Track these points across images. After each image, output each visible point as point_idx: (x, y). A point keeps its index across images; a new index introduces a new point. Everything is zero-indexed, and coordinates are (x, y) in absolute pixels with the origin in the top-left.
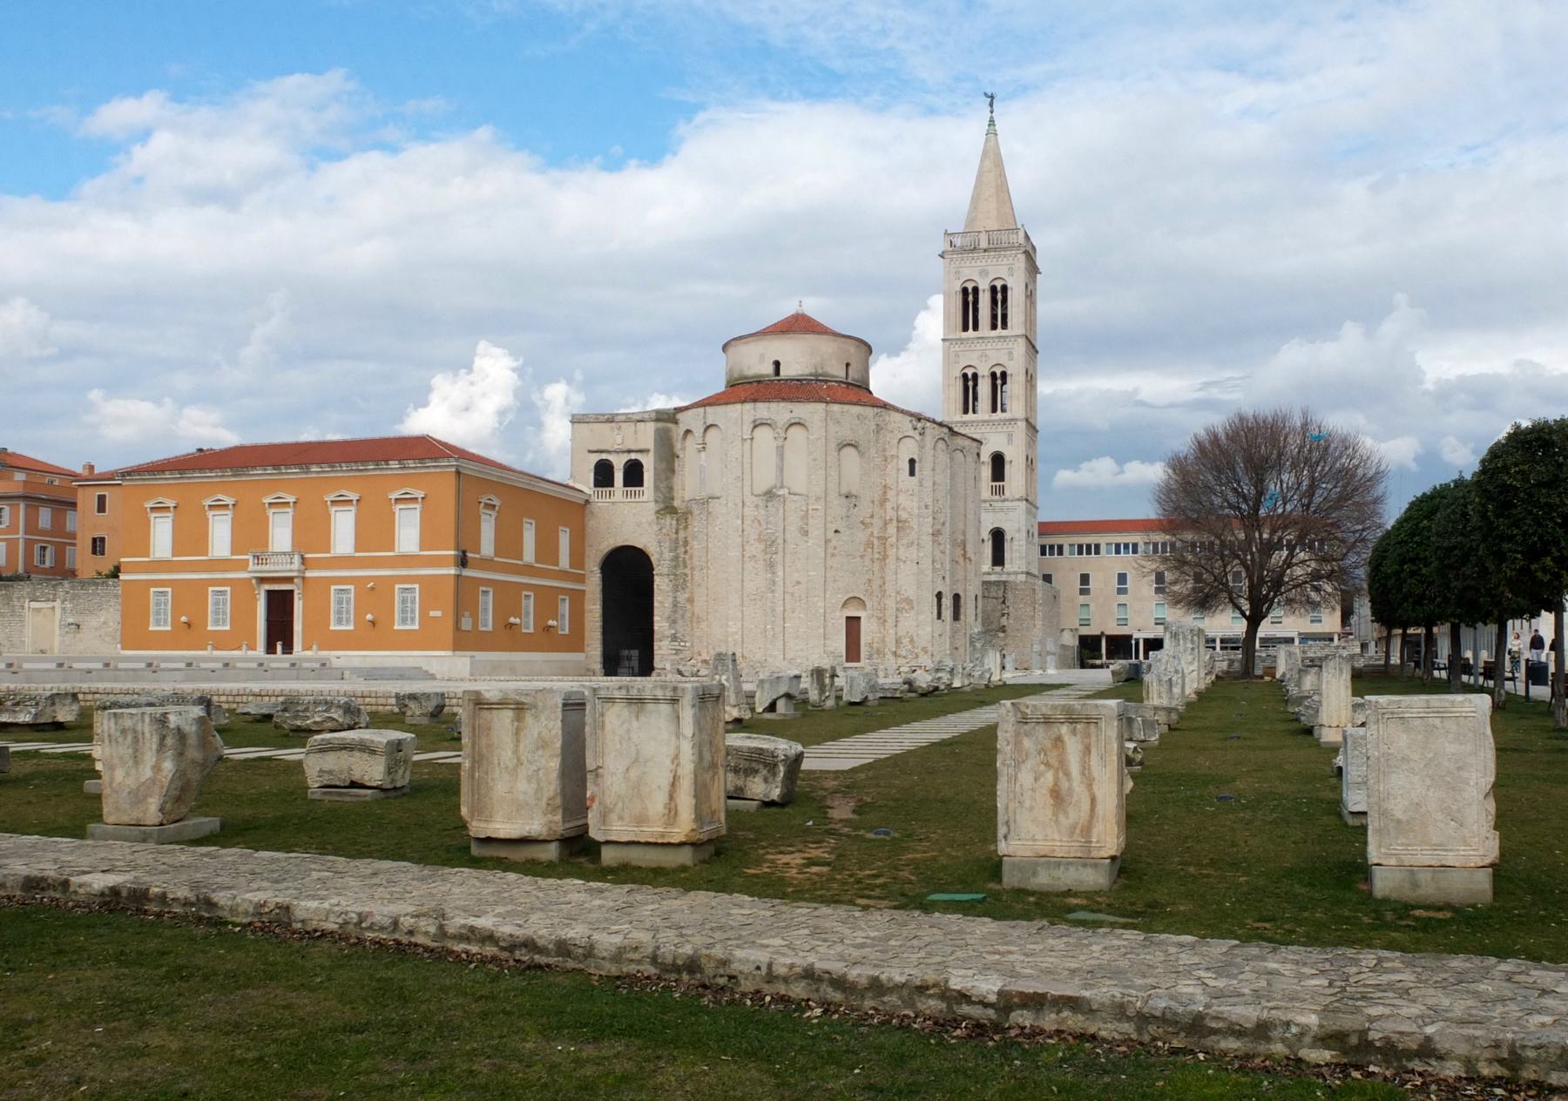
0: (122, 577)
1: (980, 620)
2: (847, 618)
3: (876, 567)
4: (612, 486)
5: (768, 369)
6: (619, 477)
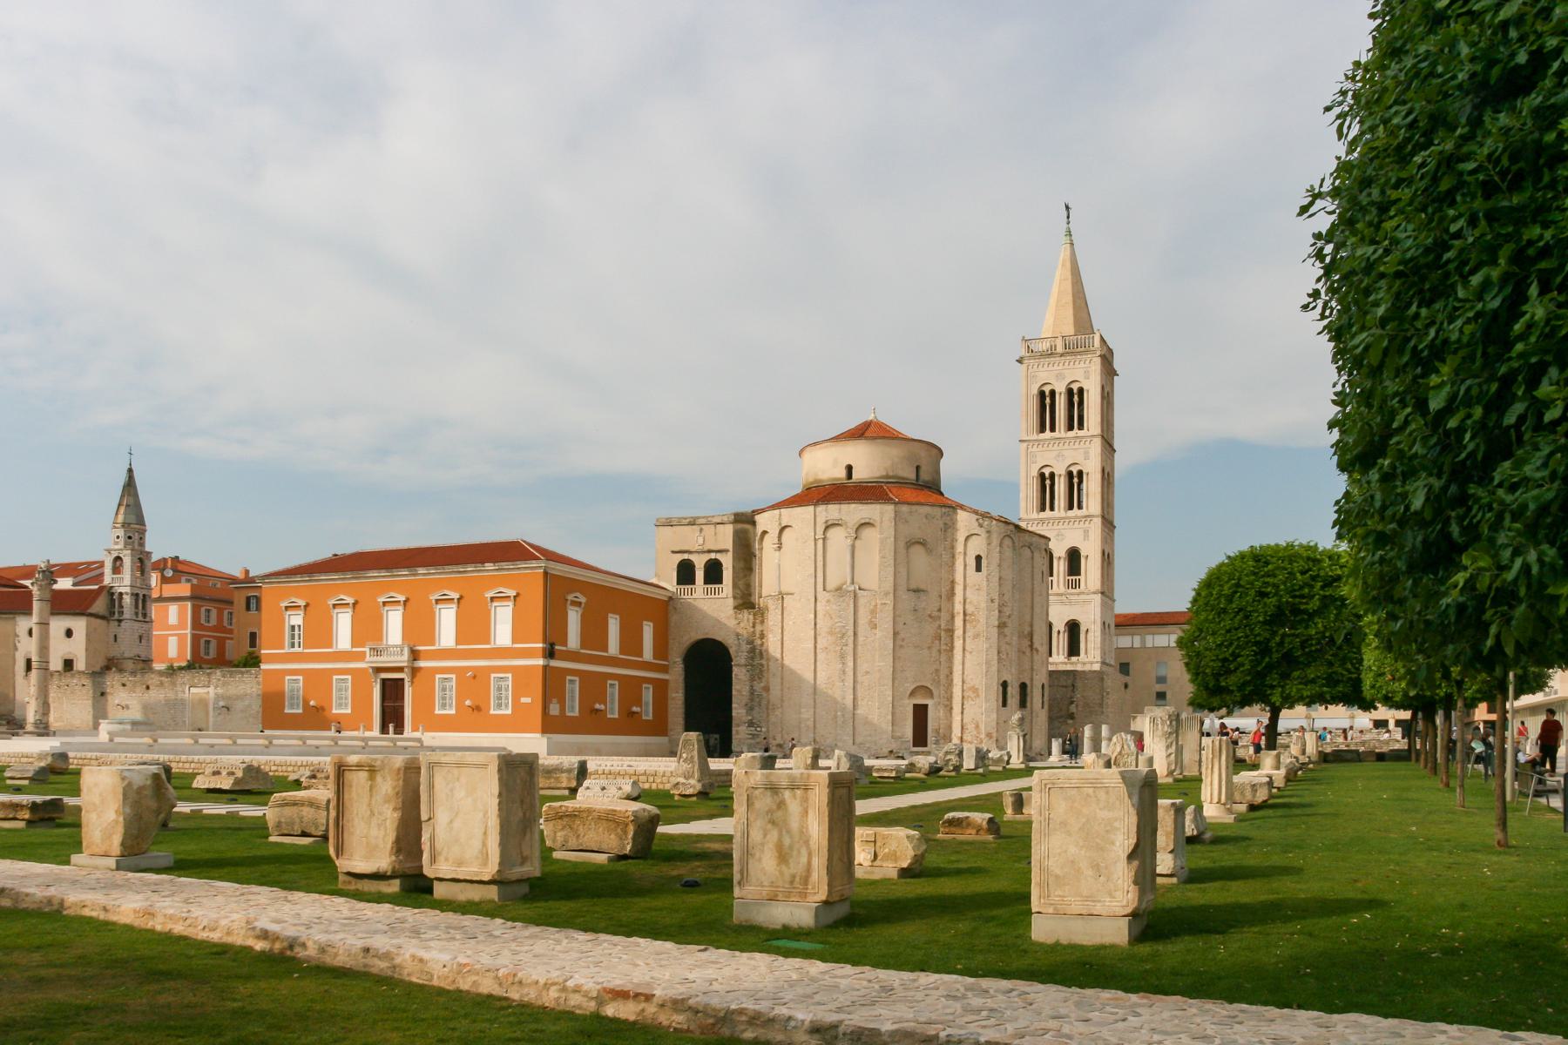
0: (263, 666)
1: (1046, 706)
2: (915, 706)
3: (943, 658)
4: (694, 583)
5: (842, 474)
6: (700, 575)
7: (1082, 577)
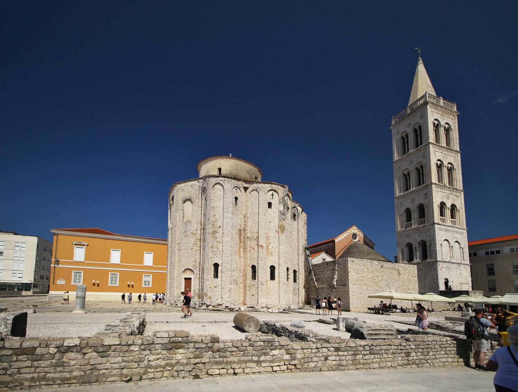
7: (426, 218)
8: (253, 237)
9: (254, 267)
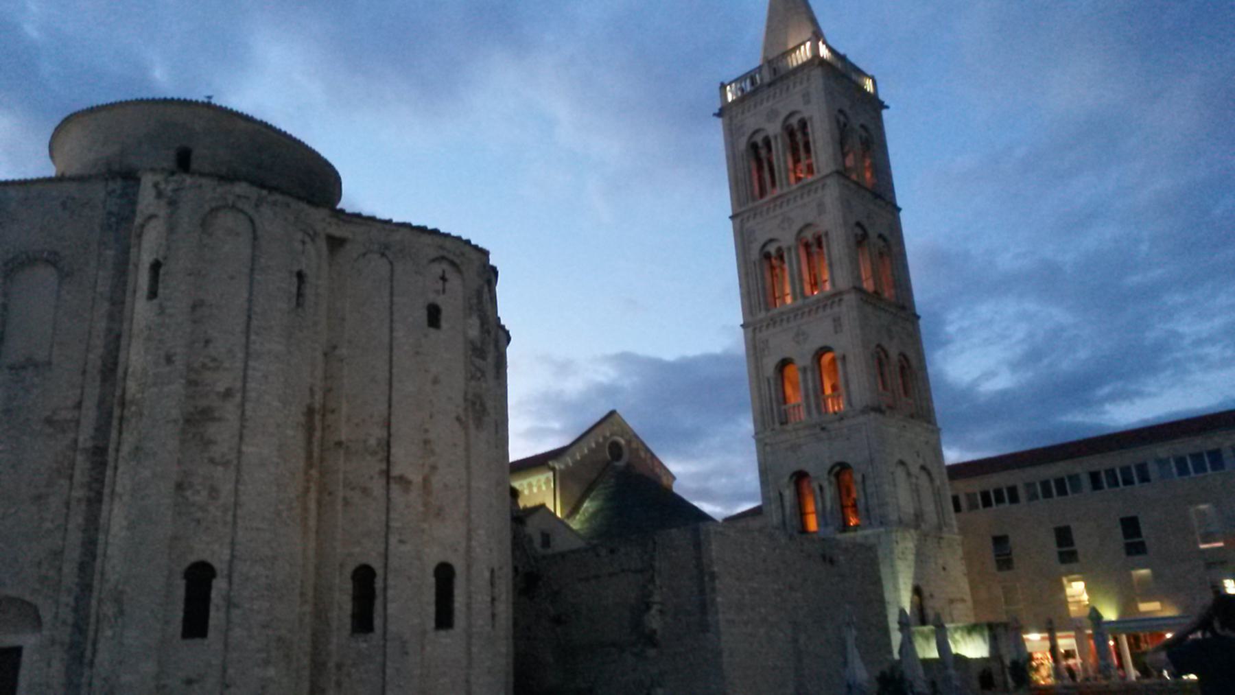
8: (365, 441)
9: (364, 580)
